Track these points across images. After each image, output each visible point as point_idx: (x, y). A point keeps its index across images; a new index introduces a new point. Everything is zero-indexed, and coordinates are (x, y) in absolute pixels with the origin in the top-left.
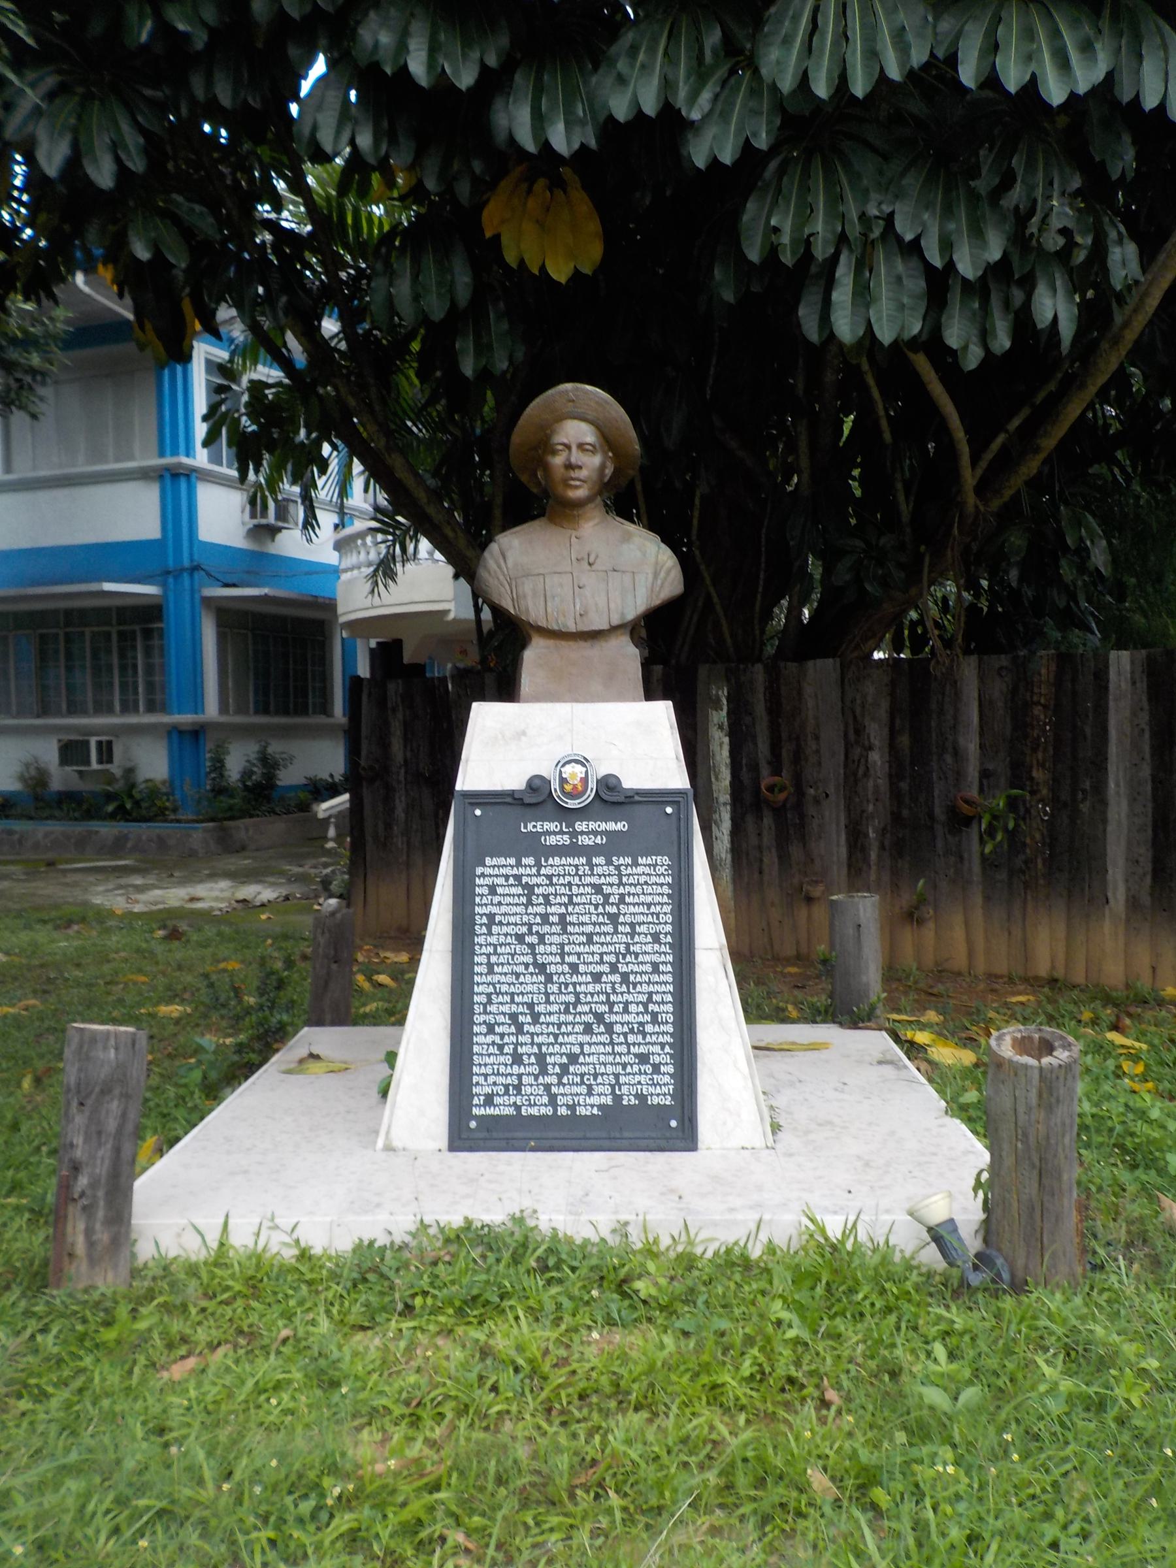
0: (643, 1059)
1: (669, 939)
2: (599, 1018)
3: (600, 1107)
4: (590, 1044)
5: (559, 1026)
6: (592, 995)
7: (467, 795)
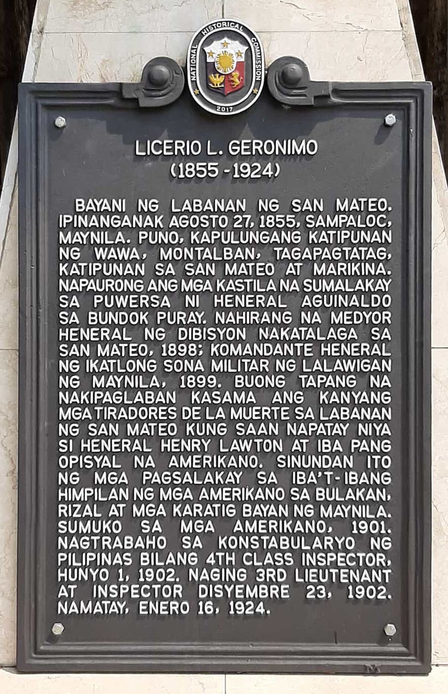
0: (343, 526)
1: (387, 334)
2: (269, 459)
3: (270, 602)
4: (253, 503)
5: (202, 471)
6: (257, 424)
7: (43, 91)
